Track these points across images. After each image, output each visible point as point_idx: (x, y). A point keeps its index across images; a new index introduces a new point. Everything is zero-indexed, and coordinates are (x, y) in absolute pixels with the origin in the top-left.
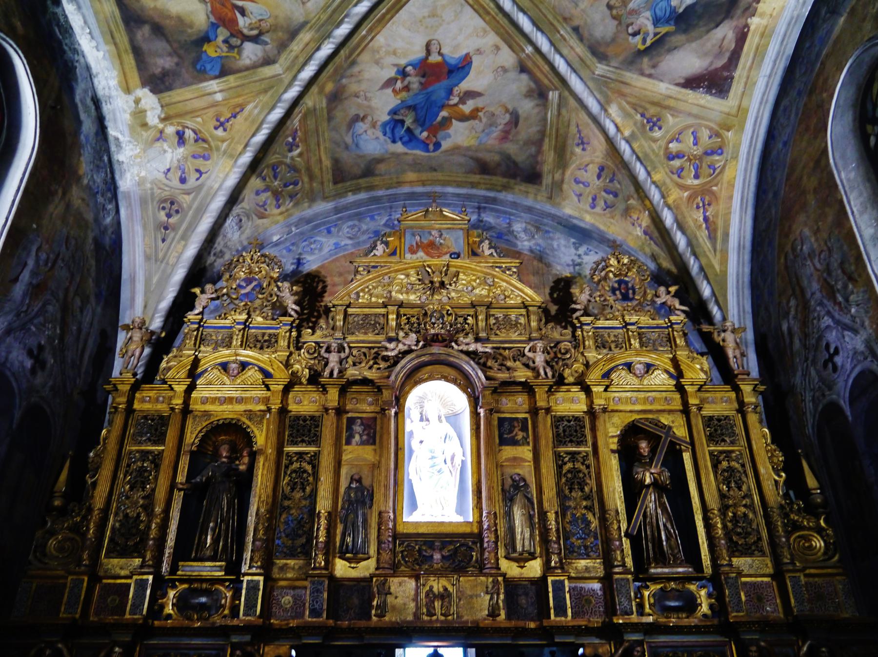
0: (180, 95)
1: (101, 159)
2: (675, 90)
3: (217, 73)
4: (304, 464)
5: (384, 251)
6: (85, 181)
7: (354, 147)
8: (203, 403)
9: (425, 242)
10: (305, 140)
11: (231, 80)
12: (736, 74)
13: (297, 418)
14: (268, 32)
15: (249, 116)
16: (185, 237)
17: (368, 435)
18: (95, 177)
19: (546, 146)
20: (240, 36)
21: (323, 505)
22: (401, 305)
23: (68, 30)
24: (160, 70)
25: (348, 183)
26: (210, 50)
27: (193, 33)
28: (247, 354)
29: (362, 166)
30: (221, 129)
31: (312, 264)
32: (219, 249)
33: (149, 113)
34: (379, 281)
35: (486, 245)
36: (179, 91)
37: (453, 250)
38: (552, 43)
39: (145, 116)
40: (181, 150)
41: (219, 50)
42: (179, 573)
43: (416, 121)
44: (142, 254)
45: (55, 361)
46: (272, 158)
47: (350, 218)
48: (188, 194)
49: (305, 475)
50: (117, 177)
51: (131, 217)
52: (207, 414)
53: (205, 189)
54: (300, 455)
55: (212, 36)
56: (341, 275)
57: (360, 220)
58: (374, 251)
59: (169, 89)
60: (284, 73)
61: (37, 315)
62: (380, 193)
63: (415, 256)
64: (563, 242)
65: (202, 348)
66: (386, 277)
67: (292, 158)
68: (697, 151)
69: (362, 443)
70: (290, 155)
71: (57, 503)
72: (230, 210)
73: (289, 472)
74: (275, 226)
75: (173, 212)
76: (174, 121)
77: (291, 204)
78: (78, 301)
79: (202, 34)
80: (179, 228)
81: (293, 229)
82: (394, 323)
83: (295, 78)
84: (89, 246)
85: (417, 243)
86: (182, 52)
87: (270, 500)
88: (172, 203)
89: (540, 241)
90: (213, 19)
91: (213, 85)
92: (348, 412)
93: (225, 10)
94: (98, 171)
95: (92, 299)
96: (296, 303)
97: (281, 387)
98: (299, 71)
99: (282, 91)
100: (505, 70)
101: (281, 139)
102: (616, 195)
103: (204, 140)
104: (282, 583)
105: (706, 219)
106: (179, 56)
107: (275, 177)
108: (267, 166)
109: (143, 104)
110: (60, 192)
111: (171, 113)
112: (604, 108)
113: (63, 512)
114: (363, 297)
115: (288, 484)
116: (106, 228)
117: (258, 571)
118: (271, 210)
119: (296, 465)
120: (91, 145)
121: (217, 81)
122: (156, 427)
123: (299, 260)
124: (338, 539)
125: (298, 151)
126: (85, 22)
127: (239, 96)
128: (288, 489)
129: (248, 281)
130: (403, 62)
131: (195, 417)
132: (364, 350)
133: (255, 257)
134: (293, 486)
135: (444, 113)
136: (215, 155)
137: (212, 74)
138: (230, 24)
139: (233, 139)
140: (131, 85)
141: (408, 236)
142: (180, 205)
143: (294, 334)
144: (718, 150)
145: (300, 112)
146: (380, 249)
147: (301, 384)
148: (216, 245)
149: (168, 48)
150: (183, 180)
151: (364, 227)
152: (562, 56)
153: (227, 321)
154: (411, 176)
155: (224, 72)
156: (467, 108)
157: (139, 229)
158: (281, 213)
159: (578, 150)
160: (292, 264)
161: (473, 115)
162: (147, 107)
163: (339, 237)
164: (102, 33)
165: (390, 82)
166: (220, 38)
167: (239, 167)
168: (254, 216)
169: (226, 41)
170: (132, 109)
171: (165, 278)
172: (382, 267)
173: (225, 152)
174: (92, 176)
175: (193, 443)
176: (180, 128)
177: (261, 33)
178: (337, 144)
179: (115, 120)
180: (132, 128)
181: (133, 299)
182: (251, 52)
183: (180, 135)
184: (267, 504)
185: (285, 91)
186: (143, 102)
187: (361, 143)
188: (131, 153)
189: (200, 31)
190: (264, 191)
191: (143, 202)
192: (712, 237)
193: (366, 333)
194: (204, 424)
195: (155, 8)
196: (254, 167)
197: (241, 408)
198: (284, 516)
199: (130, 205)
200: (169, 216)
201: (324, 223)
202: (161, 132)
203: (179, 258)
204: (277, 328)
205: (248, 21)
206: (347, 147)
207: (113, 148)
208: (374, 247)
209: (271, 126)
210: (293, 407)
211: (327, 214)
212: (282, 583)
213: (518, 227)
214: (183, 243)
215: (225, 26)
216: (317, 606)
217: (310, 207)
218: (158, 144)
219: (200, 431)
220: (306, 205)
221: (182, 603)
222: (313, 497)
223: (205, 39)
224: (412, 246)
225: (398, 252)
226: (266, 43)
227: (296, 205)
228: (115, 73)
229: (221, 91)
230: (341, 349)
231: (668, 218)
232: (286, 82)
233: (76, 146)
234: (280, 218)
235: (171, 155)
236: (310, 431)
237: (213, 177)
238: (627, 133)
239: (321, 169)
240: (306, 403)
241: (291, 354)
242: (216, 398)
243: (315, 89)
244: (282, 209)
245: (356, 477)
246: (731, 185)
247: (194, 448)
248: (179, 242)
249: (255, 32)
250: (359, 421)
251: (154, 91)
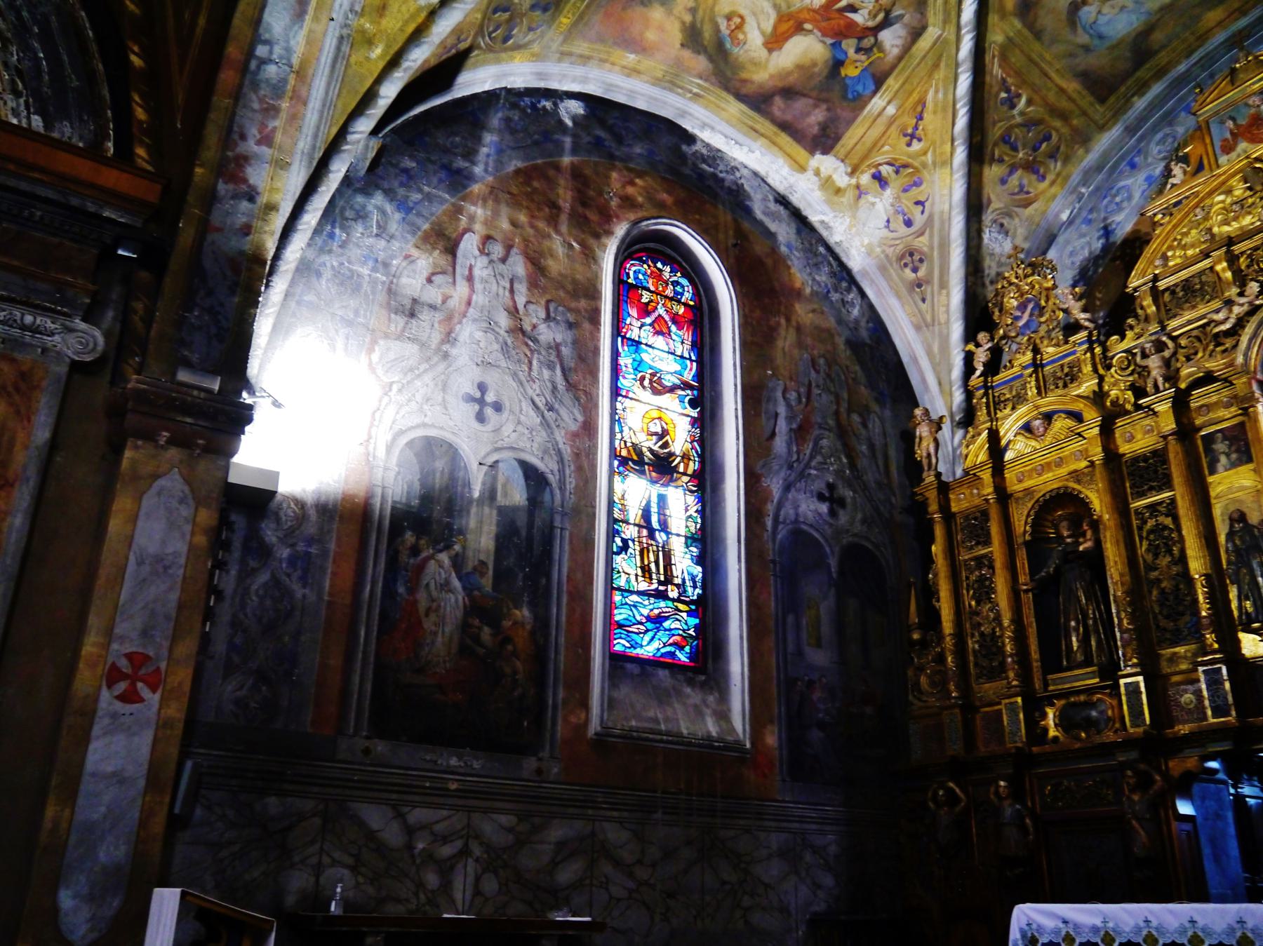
0: (853, 136)
1: (816, 254)
3: (873, 87)
4: (1161, 519)
5: (1185, 172)
6: (808, 290)
7: (1096, 42)
8: (1020, 481)
9: (1243, 121)
10: (1023, 83)
11: (892, 83)
13: (1136, 460)
14: (894, 4)
15: (936, 105)
16: (944, 285)
17: (1237, 451)
18: (818, 278)
20: (868, 33)
21: (1197, 566)
22: (1230, 241)
23: (715, 156)
24: (816, 128)
25: (1123, 89)
26: (850, 71)
27: (821, 70)
28: (1050, 402)
29: (1128, 54)
30: (915, 141)
32: (993, 273)
33: (835, 177)
34: (1190, 221)
36: (848, 134)
39: (833, 182)
40: (888, 192)
41: (858, 64)
42: (1051, 688)
44: (910, 327)
45: (855, 492)
46: (996, 132)
47: (1155, 129)
48: (922, 234)
49: (1166, 533)
50: (844, 259)
51: (879, 293)
52: (1028, 492)
53: (936, 218)
54: (1152, 507)
55: (841, 57)
57: (1170, 124)
58: (1172, 181)
59: (838, 138)
60: (944, 31)
61: (812, 457)
62: (1182, 68)
63: (1233, 155)
65: (999, 415)
66: (1198, 210)
67: (1022, 113)
69: (1234, 465)
70: (1015, 112)
71: (916, 636)
72: (980, 222)
73: (1145, 534)
74: (1055, 201)
75: (917, 264)
76: (863, 167)
77: (1059, 164)
78: (856, 418)
79: (831, 63)
80: (932, 278)
81: (1083, 190)
82: (1229, 275)
83: (959, 28)
84: (844, 352)
85: (1232, 133)
86: (824, 95)
87: (1127, 578)
88: (911, 255)
90: (829, 41)
91: (877, 103)
92: (1200, 429)
93: (833, 22)
94: (819, 269)
95: (875, 407)
96: (1084, 310)
97: (1096, 431)
98: (959, 16)
99: (954, 51)
101: (992, 103)
103: (905, 166)
104: (1175, 679)
106: (826, 101)
107: (1015, 149)
108: (996, 144)
109: (824, 172)
110: (783, 321)
111: (855, 161)
113: (924, 644)
114: (1173, 256)
115: (1148, 550)
116: (857, 321)
117: (1134, 670)
118: (1036, 188)
119: (1151, 523)
120: (797, 249)
121: (878, 95)
122: (976, 525)
123: (1105, 228)
124: (1234, 605)
125: (1023, 100)
126: (726, 137)
127: (910, 94)
128: (1149, 558)
131: (1017, 499)
132: (1195, 333)
133: (1020, 272)
134: (1154, 551)
136: (925, 174)
137: (868, 92)
138: (850, 30)
139: (933, 143)
140: (802, 162)
141: (1215, 129)
142: (921, 253)
143: (1098, 350)
145: (994, 57)
146: (1177, 170)
147: (1127, 413)
148: (987, 272)
149: (811, 101)
150: (908, 223)
151: (1180, 130)
153: (1015, 369)
157: (894, 302)
158: (1053, 183)
160: (1099, 238)
162: (829, 172)
163: (1149, 165)
164: (745, 134)
166: (851, 52)
167: (958, 171)
168: (1016, 209)
169: (858, 50)
170: (818, 183)
171: (945, 340)
172: (1187, 198)
173: (934, 163)
174: (814, 280)
175: (1025, 532)
176: (873, 170)
177: (888, 13)
178: (1072, 55)
179: (810, 205)
180: (828, 202)
181: (924, 381)
182: (891, 39)
183: (878, 177)
184: (1123, 584)
186: (822, 169)
187: (1105, 30)
188: (843, 227)
189: (826, 62)
190: (1011, 173)
191: (882, 269)
193: (1194, 307)
194: (1030, 505)
195: (772, 76)
196: (977, 156)
197: (1063, 471)
198: (1155, 593)
199: (872, 281)
200: (915, 270)
201: (1122, 158)
202: (858, 187)
203: (948, 312)
204: (1074, 353)
205: (864, 12)
206: (1086, 49)
207: (824, 233)
208: (1168, 173)
209: (965, 100)
210: (1125, 448)
211: (1117, 144)
212: (1175, 679)
214: (944, 292)
215: (846, 37)
216: (1219, 702)
217: (1087, 151)
218: (862, 201)
219: (1028, 516)
220: (1081, 152)
221: (1064, 721)
222: (1183, 560)
223: (837, 64)
224: (1226, 140)
225: (1205, 162)
226: (901, 17)
227: (1067, 160)
228: (781, 161)
229: (889, 103)
230: (1160, 347)
232: (953, 37)
233: (780, 262)
234: (1053, 190)
235: (881, 204)
236: (1156, 472)
237: (937, 199)
239: (1070, 99)
240: (1139, 436)
241: (1101, 379)
242: (1031, 470)
243: (993, 19)
244: (1050, 177)
245: (1236, 516)
247: (1028, 538)
248: (940, 293)
249: (881, 16)
250: (1219, 435)
251: (826, 152)
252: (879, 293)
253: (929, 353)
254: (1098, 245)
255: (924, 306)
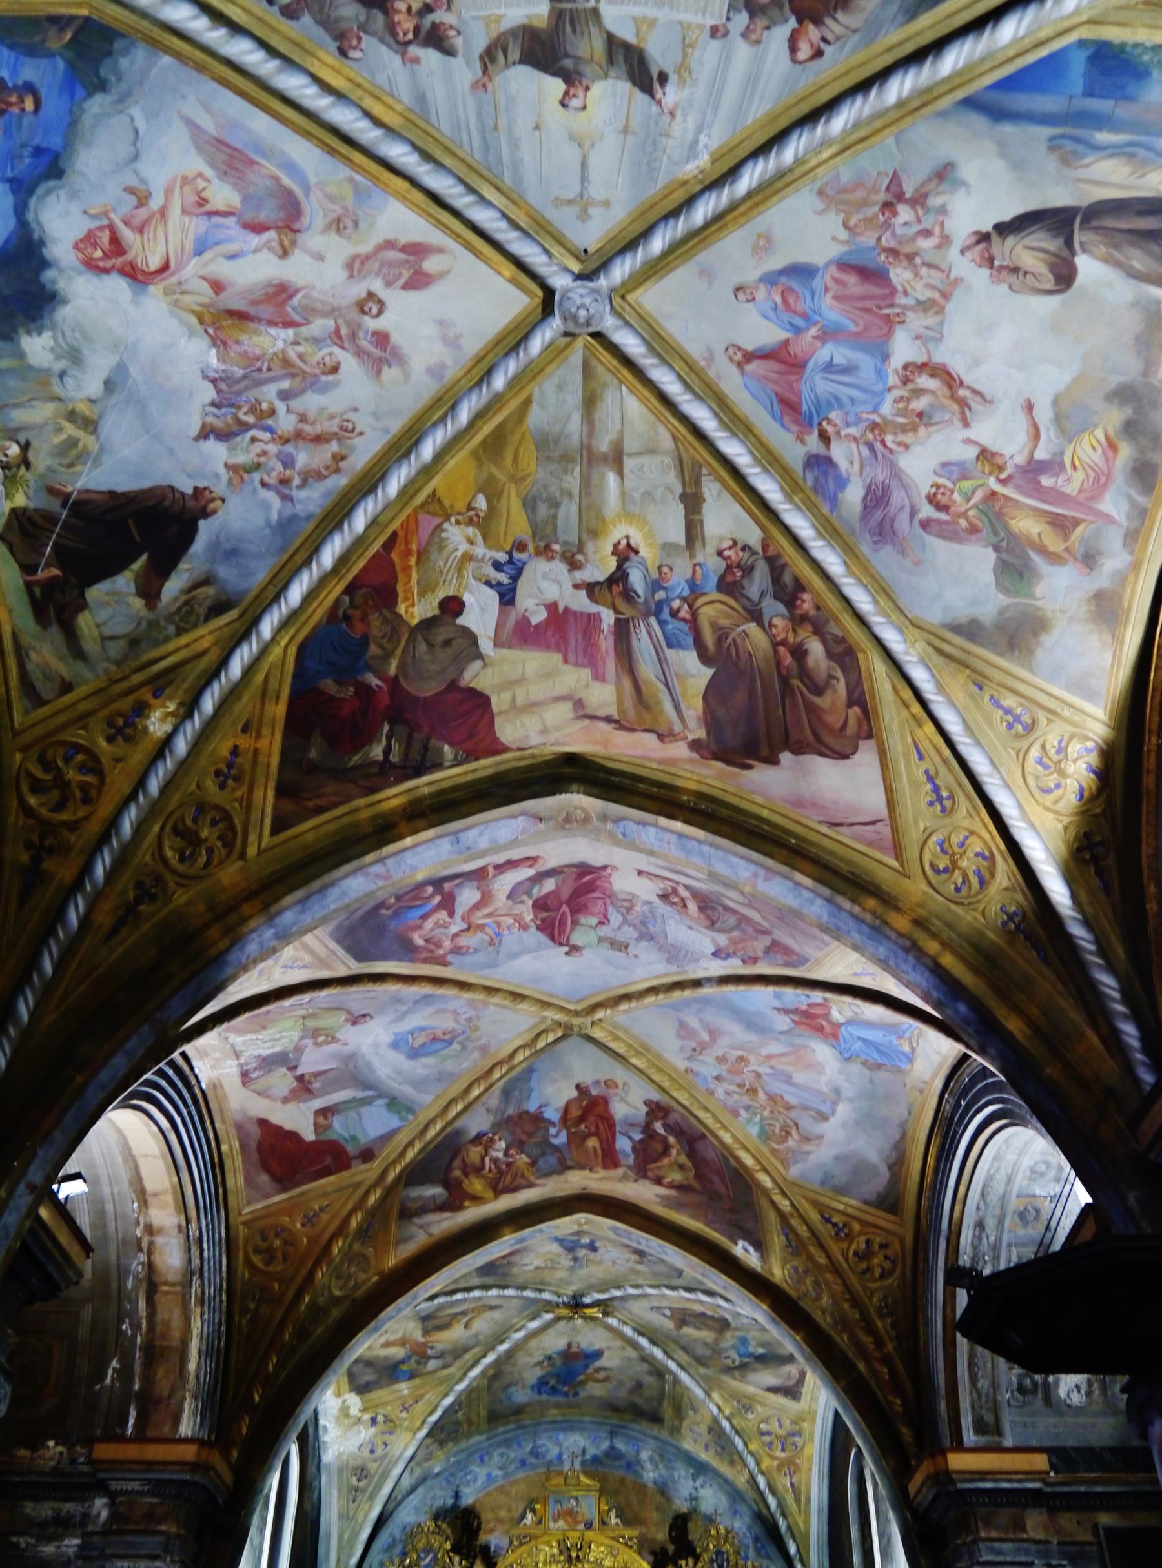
0: (378, 1395)
2: (761, 1392)
11: (417, 1381)
12: (804, 1390)
16: (372, 1498)
19: (665, 1403)
26: (404, 1367)
31: (467, 1500)
35: (613, 1514)
37: (588, 1516)
38: (665, 1352)
40: (373, 1430)
43: (558, 1382)
47: (499, 1445)
51: (329, 1483)
56: (493, 1510)
64: (683, 1472)
68: (781, 1432)
83: (465, 1374)
89: (663, 1472)
100: (629, 1359)
102: (723, 1448)
105: (792, 1485)
112: (708, 1394)
129: (428, 1550)
130: (549, 1352)
135: (582, 1377)
144: (799, 1433)
146: (529, 1516)
150: (372, 1451)
151: (512, 1455)
152: (673, 1359)
154: (554, 1412)
155: (412, 1376)
156: (601, 1375)
157: (335, 1492)
159: (691, 1413)
161: (606, 1380)
165: (540, 1364)
171: (355, 1534)
182: (432, 1364)
183: (374, 1421)
185: (457, 1383)
192: (797, 1499)
200: (359, 1480)
203: (366, 1517)
208: (523, 1516)
213: (645, 1455)
223: (403, 1362)
231: (762, 1482)
235: (365, 1434)
238: (727, 1412)
246: (810, 1460)
252: (329, 1483)
253: (340, 1538)
254: (450, 1502)
255: (351, 1505)
